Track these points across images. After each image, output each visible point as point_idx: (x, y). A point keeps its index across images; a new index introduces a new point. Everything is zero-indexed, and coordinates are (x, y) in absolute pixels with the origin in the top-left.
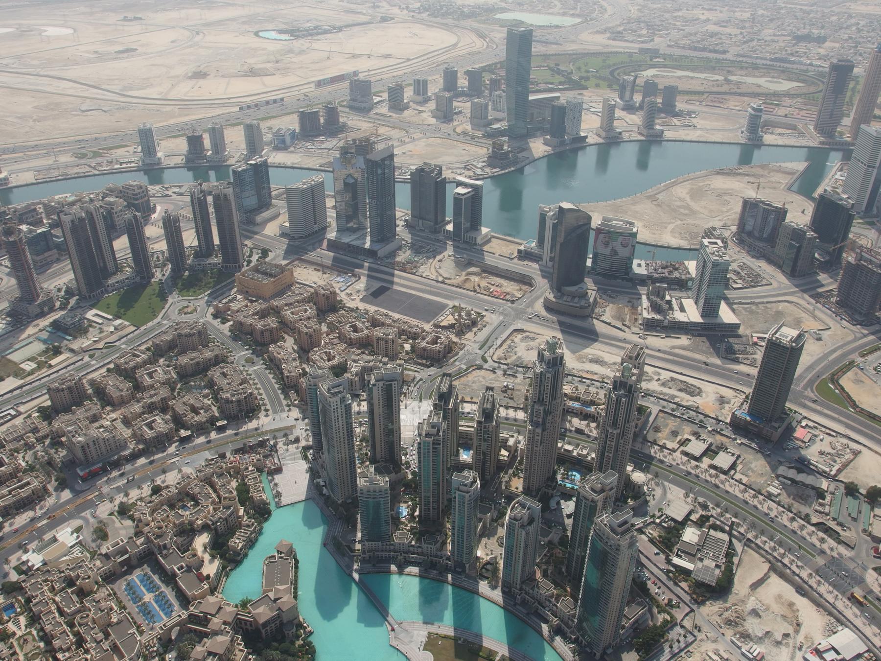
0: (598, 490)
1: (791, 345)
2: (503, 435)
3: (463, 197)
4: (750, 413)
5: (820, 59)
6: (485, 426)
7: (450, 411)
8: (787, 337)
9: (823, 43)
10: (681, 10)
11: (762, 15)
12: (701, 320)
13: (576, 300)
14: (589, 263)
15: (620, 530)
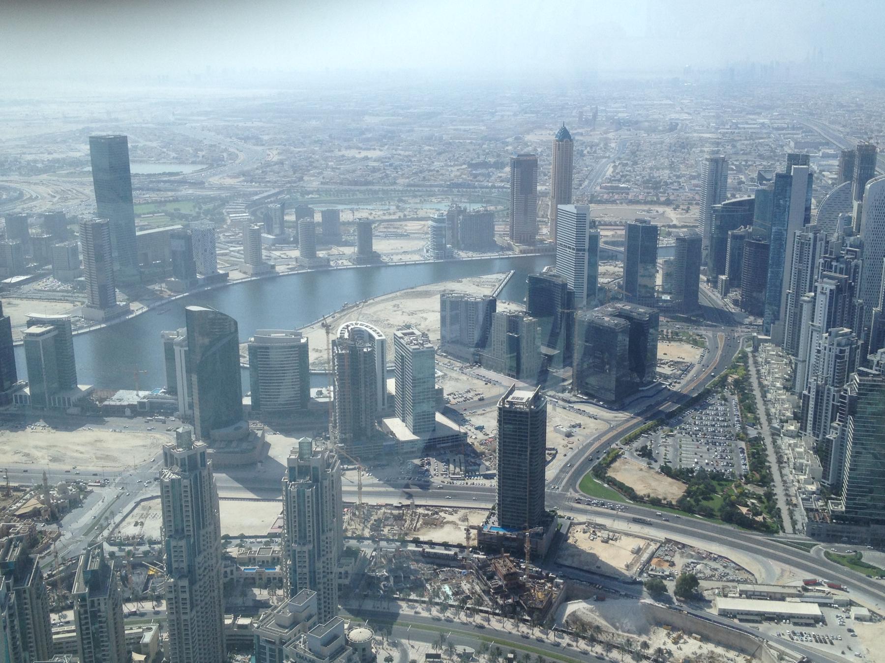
0: (287, 624)
1: (531, 409)
2: (131, 630)
3: (40, 339)
4: (504, 526)
5: (502, 181)
6: (93, 602)
7: (27, 596)
8: (522, 399)
9: (502, 169)
10: (333, 151)
11: (429, 150)
12: (415, 437)
13: (234, 444)
14: (247, 401)
15: (327, 651)
